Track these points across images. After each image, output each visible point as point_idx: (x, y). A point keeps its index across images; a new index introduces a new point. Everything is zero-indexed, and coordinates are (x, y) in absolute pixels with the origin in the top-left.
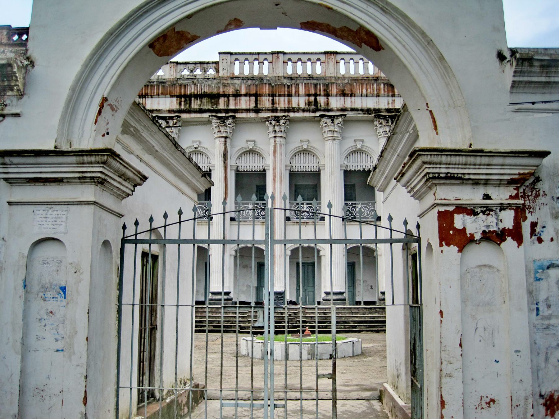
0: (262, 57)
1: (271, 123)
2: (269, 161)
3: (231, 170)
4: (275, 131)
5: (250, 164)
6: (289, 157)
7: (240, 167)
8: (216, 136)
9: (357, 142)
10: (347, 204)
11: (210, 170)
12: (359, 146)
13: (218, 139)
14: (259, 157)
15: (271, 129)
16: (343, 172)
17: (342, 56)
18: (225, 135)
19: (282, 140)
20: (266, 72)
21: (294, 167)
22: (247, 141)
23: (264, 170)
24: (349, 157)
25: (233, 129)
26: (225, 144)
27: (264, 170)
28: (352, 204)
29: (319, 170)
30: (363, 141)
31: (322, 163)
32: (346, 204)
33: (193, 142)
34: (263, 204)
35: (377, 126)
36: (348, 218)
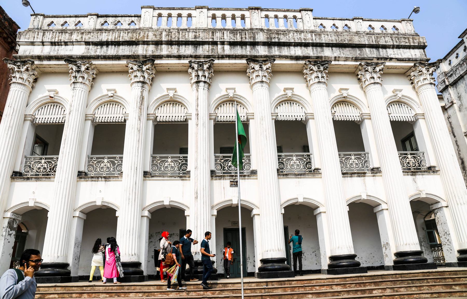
1: (193, 68)
2: (192, 110)
4: (198, 76)
6: (213, 107)
9: (287, 91)
10: (281, 156)
11: (125, 121)
15: (194, 74)
16: (274, 121)
18: (142, 79)
23: (186, 120)
26: (142, 92)
27: (186, 120)
30: (292, 89)
31: (250, 111)
32: (279, 156)
34: (184, 157)
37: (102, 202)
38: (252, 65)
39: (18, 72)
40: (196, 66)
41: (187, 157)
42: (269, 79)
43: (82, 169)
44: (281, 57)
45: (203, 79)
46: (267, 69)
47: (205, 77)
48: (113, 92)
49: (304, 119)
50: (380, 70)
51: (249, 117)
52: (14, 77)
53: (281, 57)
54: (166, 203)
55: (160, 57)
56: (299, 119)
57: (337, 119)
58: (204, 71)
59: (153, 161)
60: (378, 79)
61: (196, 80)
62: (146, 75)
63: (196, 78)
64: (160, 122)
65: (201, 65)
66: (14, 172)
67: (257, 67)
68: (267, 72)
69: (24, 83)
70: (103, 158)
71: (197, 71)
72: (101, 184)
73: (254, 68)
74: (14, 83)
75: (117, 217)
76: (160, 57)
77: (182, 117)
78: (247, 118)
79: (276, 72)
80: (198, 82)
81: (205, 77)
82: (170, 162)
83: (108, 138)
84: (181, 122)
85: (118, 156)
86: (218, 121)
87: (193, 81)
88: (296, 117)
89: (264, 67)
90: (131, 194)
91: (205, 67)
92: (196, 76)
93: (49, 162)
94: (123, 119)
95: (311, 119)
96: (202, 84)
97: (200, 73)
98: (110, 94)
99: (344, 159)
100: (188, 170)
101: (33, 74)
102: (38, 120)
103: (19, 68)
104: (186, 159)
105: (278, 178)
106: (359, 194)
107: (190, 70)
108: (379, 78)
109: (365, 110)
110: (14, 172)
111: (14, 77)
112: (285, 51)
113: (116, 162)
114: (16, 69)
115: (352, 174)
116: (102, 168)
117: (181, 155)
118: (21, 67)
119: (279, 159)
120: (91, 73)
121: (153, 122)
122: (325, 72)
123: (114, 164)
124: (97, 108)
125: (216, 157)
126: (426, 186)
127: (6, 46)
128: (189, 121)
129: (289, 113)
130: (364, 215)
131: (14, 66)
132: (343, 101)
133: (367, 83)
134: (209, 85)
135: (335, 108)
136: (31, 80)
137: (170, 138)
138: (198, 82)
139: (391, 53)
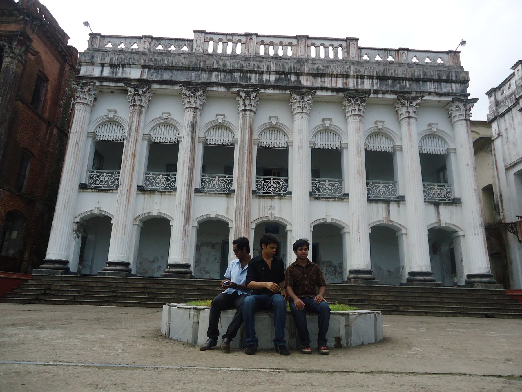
0: (235, 39)
1: (241, 97)
2: (238, 136)
3: (199, 142)
5: (219, 138)
7: (209, 140)
8: (185, 107)
9: (325, 121)
10: (315, 180)
11: (178, 142)
12: (327, 125)
13: (188, 110)
14: (228, 132)
15: (241, 103)
17: (313, 41)
18: (194, 106)
19: (252, 113)
20: (239, 51)
21: (262, 143)
22: (217, 115)
23: (233, 144)
24: (317, 136)
25: (204, 103)
28: (319, 181)
29: (288, 146)
30: (330, 120)
32: (312, 180)
33: (163, 113)
34: (229, 177)
35: (345, 106)
36: (315, 195)
37: (159, 213)
38: (295, 96)
39: (82, 92)
40: (243, 95)
41: (232, 177)
42: (309, 109)
43: (141, 184)
44: (322, 89)
45: (249, 108)
46: (308, 100)
47: (251, 105)
48: (168, 115)
49: (339, 148)
50: (416, 105)
51: (289, 144)
52: (78, 97)
53: (322, 89)
54: (213, 216)
55: (212, 84)
56: (334, 148)
57: (370, 149)
58: (251, 100)
59: (202, 179)
60: (413, 113)
61: (243, 108)
62: (198, 102)
63: (243, 106)
64: (210, 144)
65: (248, 94)
66: (80, 183)
67: (298, 98)
68: (309, 103)
70: (159, 175)
71: (244, 100)
72: (157, 197)
73: (296, 99)
74: (78, 102)
75: (171, 226)
76: (212, 84)
77: (230, 141)
78: (287, 144)
79: (317, 102)
80: (245, 110)
81: (251, 105)
82: (217, 181)
83: (163, 157)
84: (228, 145)
85: (171, 173)
86: (261, 147)
87: (240, 109)
88: (332, 146)
89: (306, 100)
90: (182, 207)
91: (253, 95)
92: (243, 104)
93: (110, 176)
94: (177, 140)
95: (345, 148)
96: (248, 113)
97: (247, 102)
98: (165, 116)
99: (372, 186)
100: (233, 188)
102: (99, 137)
103: (82, 89)
104: (231, 179)
105: (310, 200)
106: (381, 219)
107: (238, 98)
108: (415, 112)
109: (398, 143)
111: (78, 97)
112: (327, 82)
113: (170, 178)
114: (79, 90)
115: (377, 201)
116: (158, 183)
117: (227, 176)
118: (84, 88)
119: (313, 183)
120: (148, 96)
121: (203, 144)
122: (363, 105)
123: (168, 180)
124: (153, 128)
125: (257, 178)
126: (448, 217)
128: (235, 145)
129: (326, 142)
130: (385, 238)
131: (78, 87)
132: (378, 133)
133: (403, 117)
134: (255, 113)
135: (369, 139)
136: (92, 100)
137: (218, 160)
138: (245, 110)
139: (430, 87)
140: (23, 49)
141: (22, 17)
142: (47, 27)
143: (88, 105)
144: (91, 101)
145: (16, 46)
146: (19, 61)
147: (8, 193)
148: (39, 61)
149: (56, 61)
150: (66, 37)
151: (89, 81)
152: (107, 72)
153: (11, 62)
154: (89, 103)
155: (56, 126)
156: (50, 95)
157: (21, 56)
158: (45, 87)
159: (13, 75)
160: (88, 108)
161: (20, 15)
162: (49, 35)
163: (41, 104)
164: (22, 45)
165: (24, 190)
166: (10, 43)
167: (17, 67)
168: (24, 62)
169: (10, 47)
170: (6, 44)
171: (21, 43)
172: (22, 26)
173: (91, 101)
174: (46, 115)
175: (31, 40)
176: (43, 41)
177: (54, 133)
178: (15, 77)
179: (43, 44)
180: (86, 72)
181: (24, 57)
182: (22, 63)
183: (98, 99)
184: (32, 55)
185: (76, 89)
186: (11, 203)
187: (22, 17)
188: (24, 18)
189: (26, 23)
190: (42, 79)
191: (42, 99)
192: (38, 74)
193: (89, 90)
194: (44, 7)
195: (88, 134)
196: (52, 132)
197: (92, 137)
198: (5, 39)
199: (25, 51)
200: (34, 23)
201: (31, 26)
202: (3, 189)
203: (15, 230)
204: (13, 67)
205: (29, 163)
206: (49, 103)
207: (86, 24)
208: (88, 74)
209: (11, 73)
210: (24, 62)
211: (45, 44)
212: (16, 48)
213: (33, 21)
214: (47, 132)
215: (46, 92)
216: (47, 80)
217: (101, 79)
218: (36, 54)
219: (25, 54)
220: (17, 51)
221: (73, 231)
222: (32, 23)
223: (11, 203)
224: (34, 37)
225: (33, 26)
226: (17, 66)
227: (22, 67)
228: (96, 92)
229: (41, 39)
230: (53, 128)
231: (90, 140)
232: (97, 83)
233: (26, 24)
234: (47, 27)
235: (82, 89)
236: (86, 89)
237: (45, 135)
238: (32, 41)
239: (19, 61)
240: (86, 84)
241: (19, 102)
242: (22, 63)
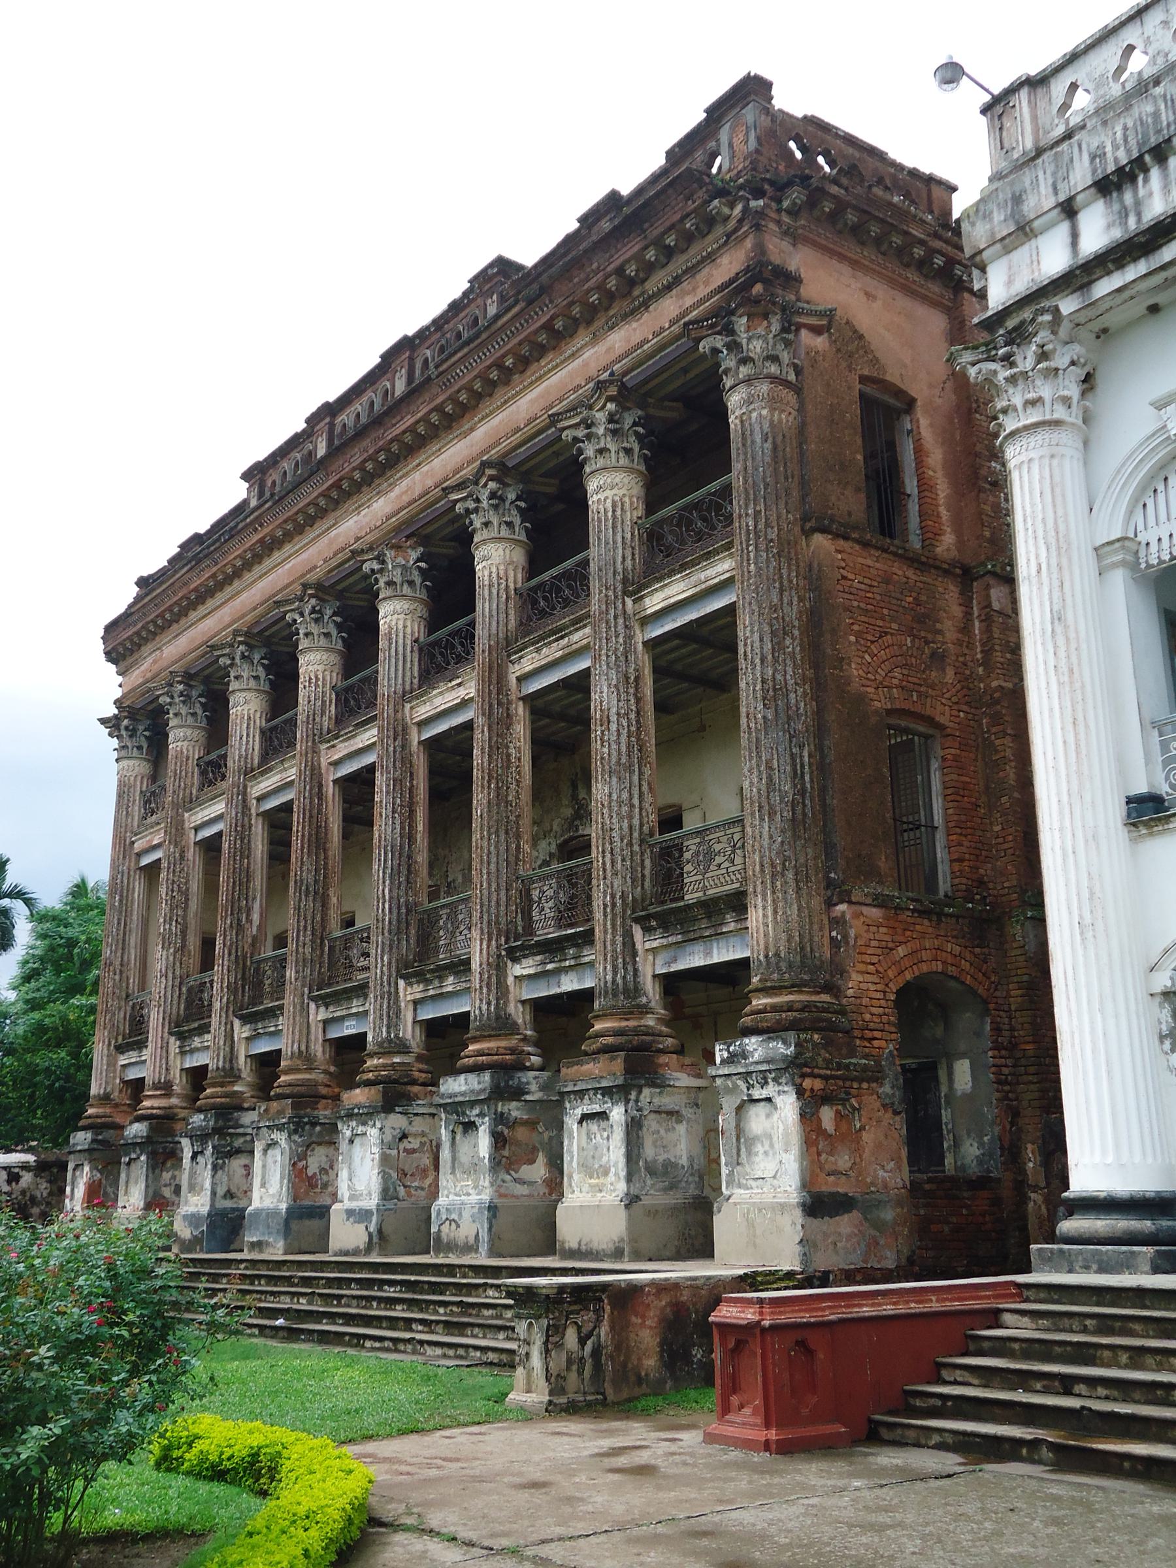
39: (1012, 380)
52: (1005, 411)
66: (1130, 800)
69: (1048, 417)
74: (1012, 434)
101: (1073, 363)
102: (1154, 548)
103: (1012, 365)
110: (1130, 800)
114: (1003, 374)
118: (1018, 358)
127: (935, 288)
131: (992, 366)
140: (776, 327)
141: (739, 208)
142: (834, 190)
143: (1057, 423)
144: (1066, 401)
145: (748, 329)
146: (773, 379)
147: (875, 913)
148: (850, 341)
149: (922, 311)
150: (937, 192)
151: (1027, 314)
152: (1097, 230)
153: (749, 401)
154: (1060, 413)
155: (993, 574)
156: (936, 457)
157: (775, 359)
158: (909, 432)
159: (768, 445)
160: (1067, 440)
161: (732, 206)
162: (851, 217)
163: (913, 507)
164: (766, 316)
165: (944, 885)
166: (729, 330)
167: (772, 410)
168: (792, 377)
169: (734, 346)
170: (719, 342)
171: (759, 311)
172: (749, 243)
173: (1066, 401)
174: (947, 544)
175: (791, 280)
176: (842, 258)
177: (996, 606)
178: (775, 448)
179: (846, 269)
180: (1010, 282)
181: (785, 357)
182: (786, 383)
183: (1099, 379)
184: (817, 331)
185: (989, 380)
186: (902, 951)
187: (739, 208)
188: (746, 209)
189: (756, 221)
190: (884, 411)
191: (911, 486)
192: (862, 395)
193: (1043, 356)
194: (814, 123)
195: (1099, 558)
196: (989, 605)
197: (1123, 563)
198: (713, 326)
199: (785, 330)
200: (786, 204)
201: (779, 223)
202: (850, 902)
203: (963, 1056)
204: (761, 413)
205: (935, 765)
206: (943, 490)
207: (951, 73)
208: (1022, 286)
209: (758, 438)
210: (792, 377)
211: (855, 264)
212: (749, 339)
213: (779, 201)
214: (968, 614)
215: (919, 451)
216: (910, 404)
217: (1079, 277)
218: (827, 322)
219: (788, 344)
220: (756, 348)
221: (1162, 1038)
222: (779, 211)
223: (902, 951)
224: (797, 259)
225: (786, 219)
226: (773, 402)
227: (790, 397)
228: (1076, 350)
229: (832, 253)
230: (988, 587)
231: (1119, 579)
232: (1068, 305)
233: (757, 227)
234: (834, 190)
235: (1012, 365)
236: (1026, 359)
237: (965, 629)
238: (798, 280)
239: (773, 379)
240: (1019, 336)
241: (819, 539)
242: (786, 383)
